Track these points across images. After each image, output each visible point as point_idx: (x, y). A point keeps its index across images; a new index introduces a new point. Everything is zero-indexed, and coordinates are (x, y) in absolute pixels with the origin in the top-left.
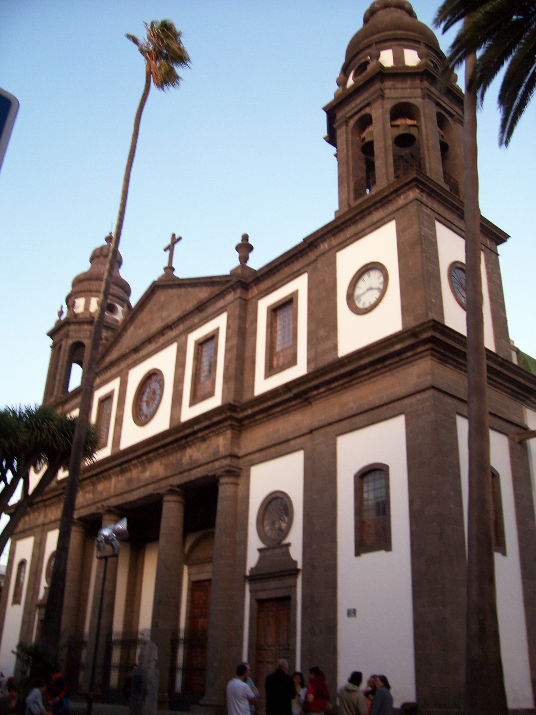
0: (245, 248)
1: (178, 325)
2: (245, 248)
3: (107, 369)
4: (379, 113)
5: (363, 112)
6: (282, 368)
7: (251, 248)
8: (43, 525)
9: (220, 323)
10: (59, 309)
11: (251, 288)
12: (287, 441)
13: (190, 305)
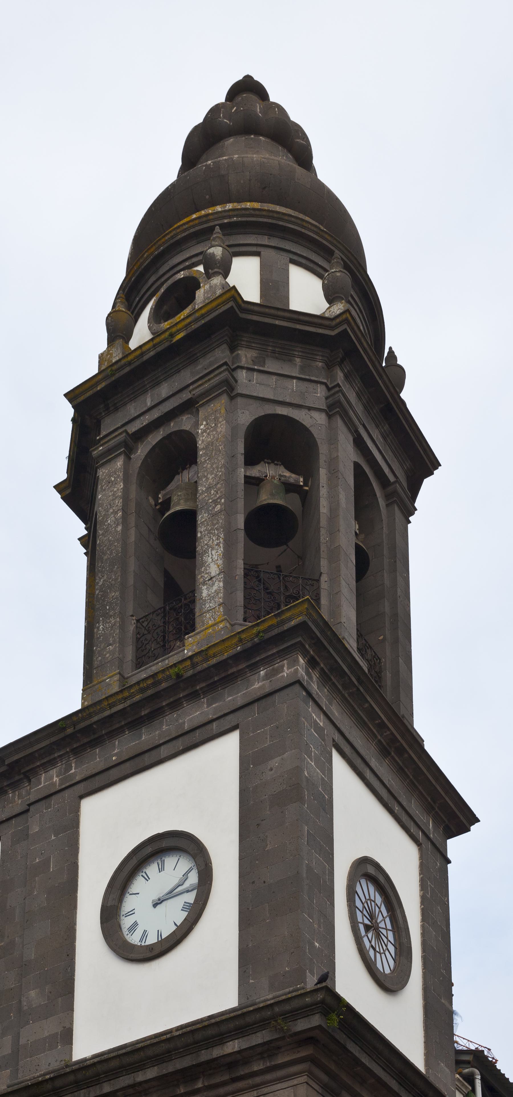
4: (216, 432)
5: (173, 426)
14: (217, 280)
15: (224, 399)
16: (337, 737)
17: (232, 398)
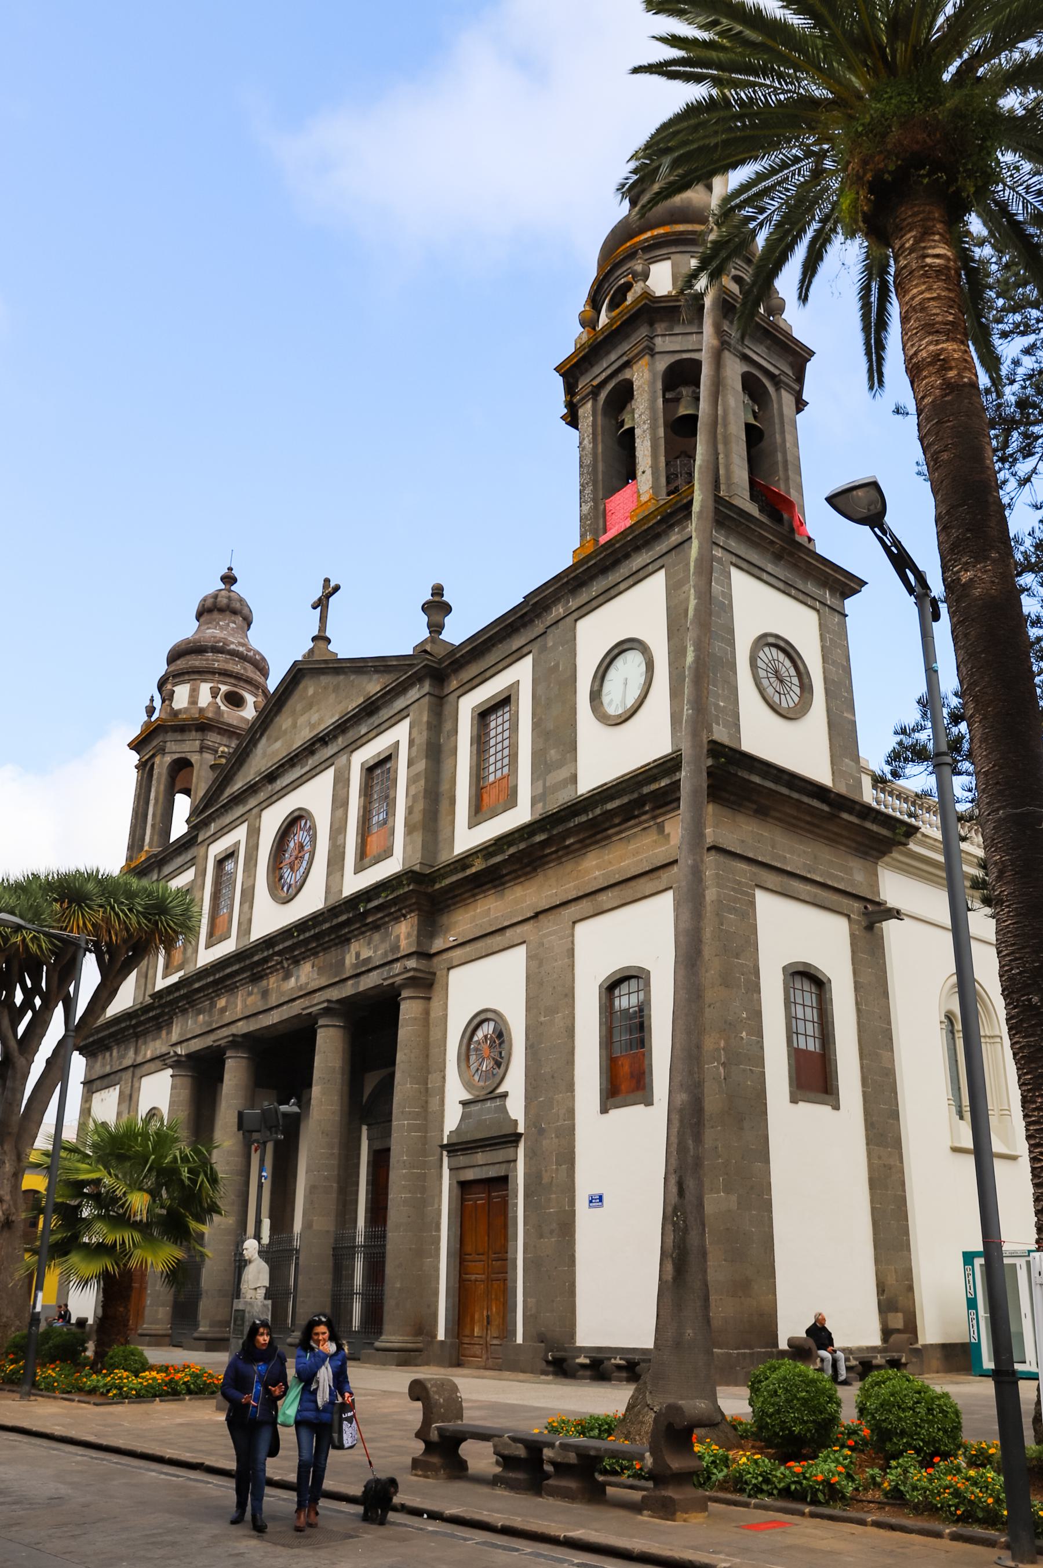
0: (437, 608)
1: (335, 737)
2: (437, 608)
3: (227, 808)
4: (644, 378)
7: (447, 609)
8: (135, 1066)
9: (400, 733)
10: (148, 703)
13: (353, 703)
14: (641, 284)
15: (647, 358)
17: (652, 356)
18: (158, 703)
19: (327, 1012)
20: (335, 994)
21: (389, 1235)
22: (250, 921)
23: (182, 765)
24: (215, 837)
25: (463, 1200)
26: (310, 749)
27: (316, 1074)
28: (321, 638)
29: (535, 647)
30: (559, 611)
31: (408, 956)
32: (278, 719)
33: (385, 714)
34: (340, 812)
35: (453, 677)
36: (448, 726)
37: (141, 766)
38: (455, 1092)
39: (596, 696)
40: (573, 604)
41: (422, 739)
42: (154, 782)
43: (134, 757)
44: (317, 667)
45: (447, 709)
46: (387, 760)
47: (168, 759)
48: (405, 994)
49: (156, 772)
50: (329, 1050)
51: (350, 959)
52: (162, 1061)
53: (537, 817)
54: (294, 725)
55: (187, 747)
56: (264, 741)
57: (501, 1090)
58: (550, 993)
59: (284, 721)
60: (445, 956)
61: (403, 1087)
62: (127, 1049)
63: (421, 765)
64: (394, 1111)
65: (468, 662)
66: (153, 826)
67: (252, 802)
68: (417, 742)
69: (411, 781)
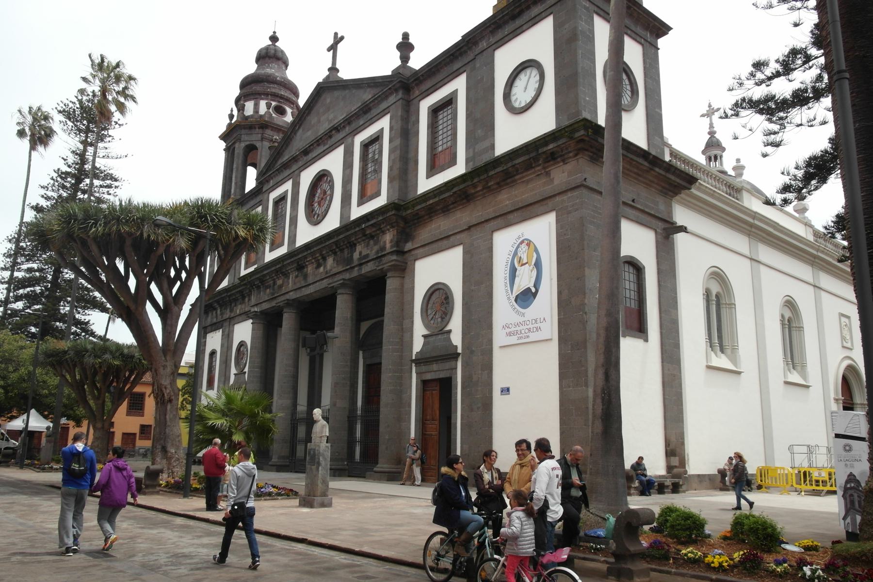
0: (405, 47)
1: (344, 127)
2: (405, 47)
6: (443, 169)
7: (411, 47)
9: (384, 123)
11: (413, 88)
12: (448, 237)
13: (354, 107)
16: (596, 9)
18: (235, 113)
19: (343, 285)
20: (347, 276)
21: (381, 409)
22: (295, 235)
23: (251, 149)
24: (273, 188)
25: (424, 391)
26: (328, 135)
27: (337, 321)
28: (333, 69)
29: (468, 68)
30: (483, 44)
31: (391, 253)
32: (309, 118)
33: (374, 112)
34: (348, 171)
35: (416, 88)
36: (413, 119)
37: (227, 150)
38: (419, 330)
39: (507, 96)
40: (492, 40)
41: (398, 126)
42: (235, 158)
43: (223, 145)
44: (331, 86)
45: (412, 108)
46: (377, 139)
47: (243, 145)
48: (389, 274)
49: (236, 152)
50: (344, 307)
51: (356, 255)
52: (246, 315)
53: (470, 170)
54: (319, 121)
55: (254, 138)
56: (301, 131)
57: (447, 328)
58: (478, 273)
59: (312, 119)
60: (413, 253)
61: (389, 327)
62: (226, 309)
63: (398, 142)
64: (384, 341)
65: (425, 80)
66: (236, 183)
67: (294, 167)
68: (395, 128)
69: (391, 151)
